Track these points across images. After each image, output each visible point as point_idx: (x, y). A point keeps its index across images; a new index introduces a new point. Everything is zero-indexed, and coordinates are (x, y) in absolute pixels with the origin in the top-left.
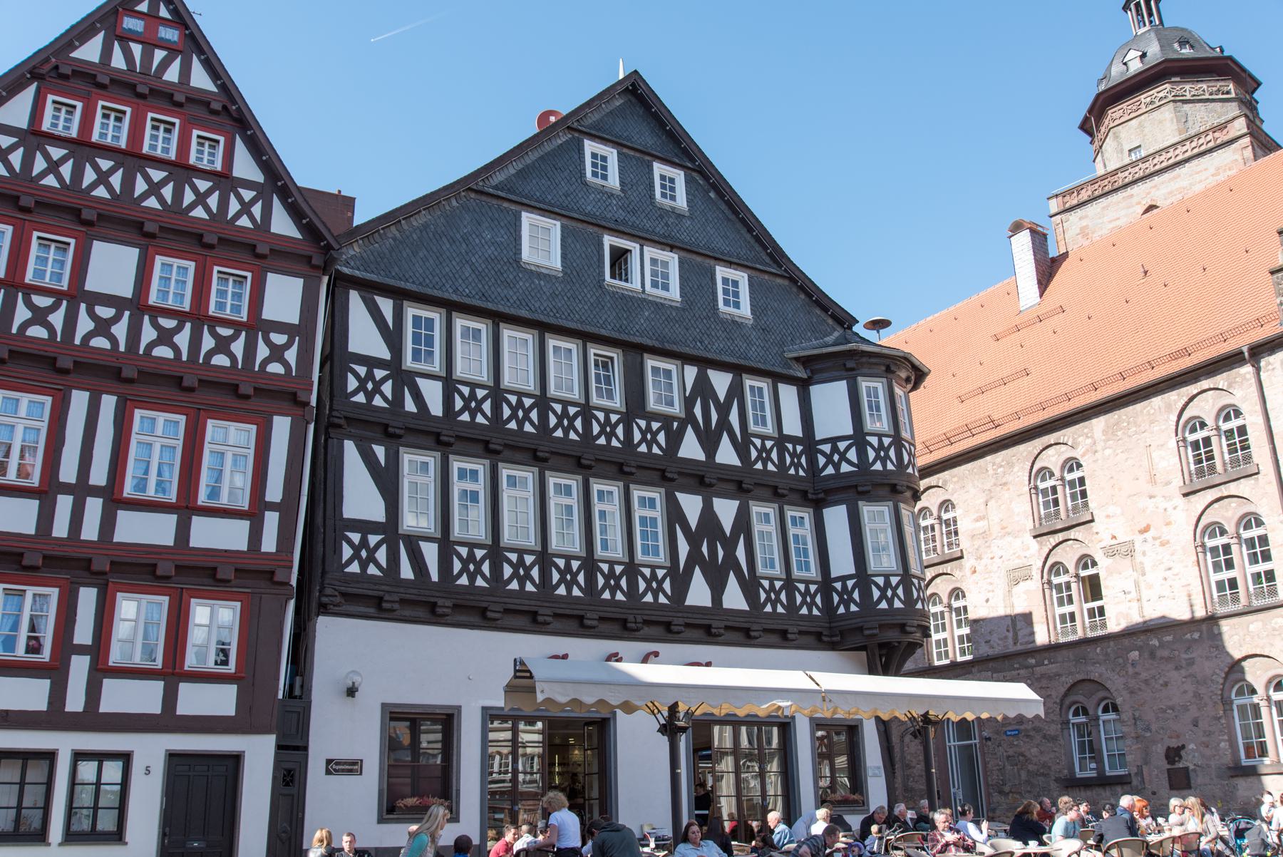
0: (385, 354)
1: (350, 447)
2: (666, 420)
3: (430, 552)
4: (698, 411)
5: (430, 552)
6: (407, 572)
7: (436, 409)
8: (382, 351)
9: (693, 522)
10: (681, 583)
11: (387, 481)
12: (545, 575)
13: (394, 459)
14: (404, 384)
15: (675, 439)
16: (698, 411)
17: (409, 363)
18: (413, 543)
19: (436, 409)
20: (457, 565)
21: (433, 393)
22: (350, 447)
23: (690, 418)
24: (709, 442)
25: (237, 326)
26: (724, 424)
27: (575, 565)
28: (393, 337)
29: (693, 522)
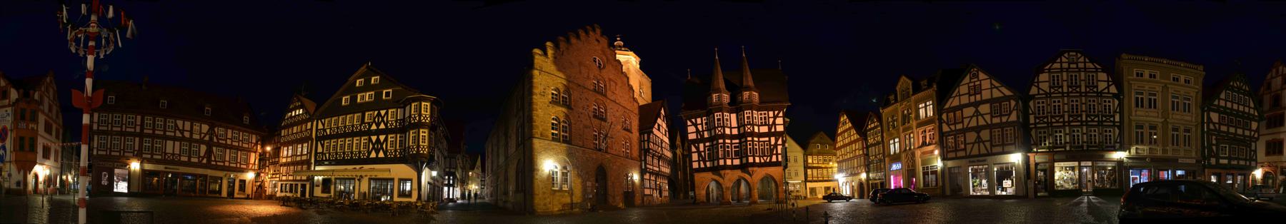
2: (369, 123)
4: (376, 120)
9: (374, 141)
10: (369, 153)
15: (370, 126)
16: (376, 120)
23: (374, 121)
24: (378, 125)
26: (383, 120)
29: (374, 141)
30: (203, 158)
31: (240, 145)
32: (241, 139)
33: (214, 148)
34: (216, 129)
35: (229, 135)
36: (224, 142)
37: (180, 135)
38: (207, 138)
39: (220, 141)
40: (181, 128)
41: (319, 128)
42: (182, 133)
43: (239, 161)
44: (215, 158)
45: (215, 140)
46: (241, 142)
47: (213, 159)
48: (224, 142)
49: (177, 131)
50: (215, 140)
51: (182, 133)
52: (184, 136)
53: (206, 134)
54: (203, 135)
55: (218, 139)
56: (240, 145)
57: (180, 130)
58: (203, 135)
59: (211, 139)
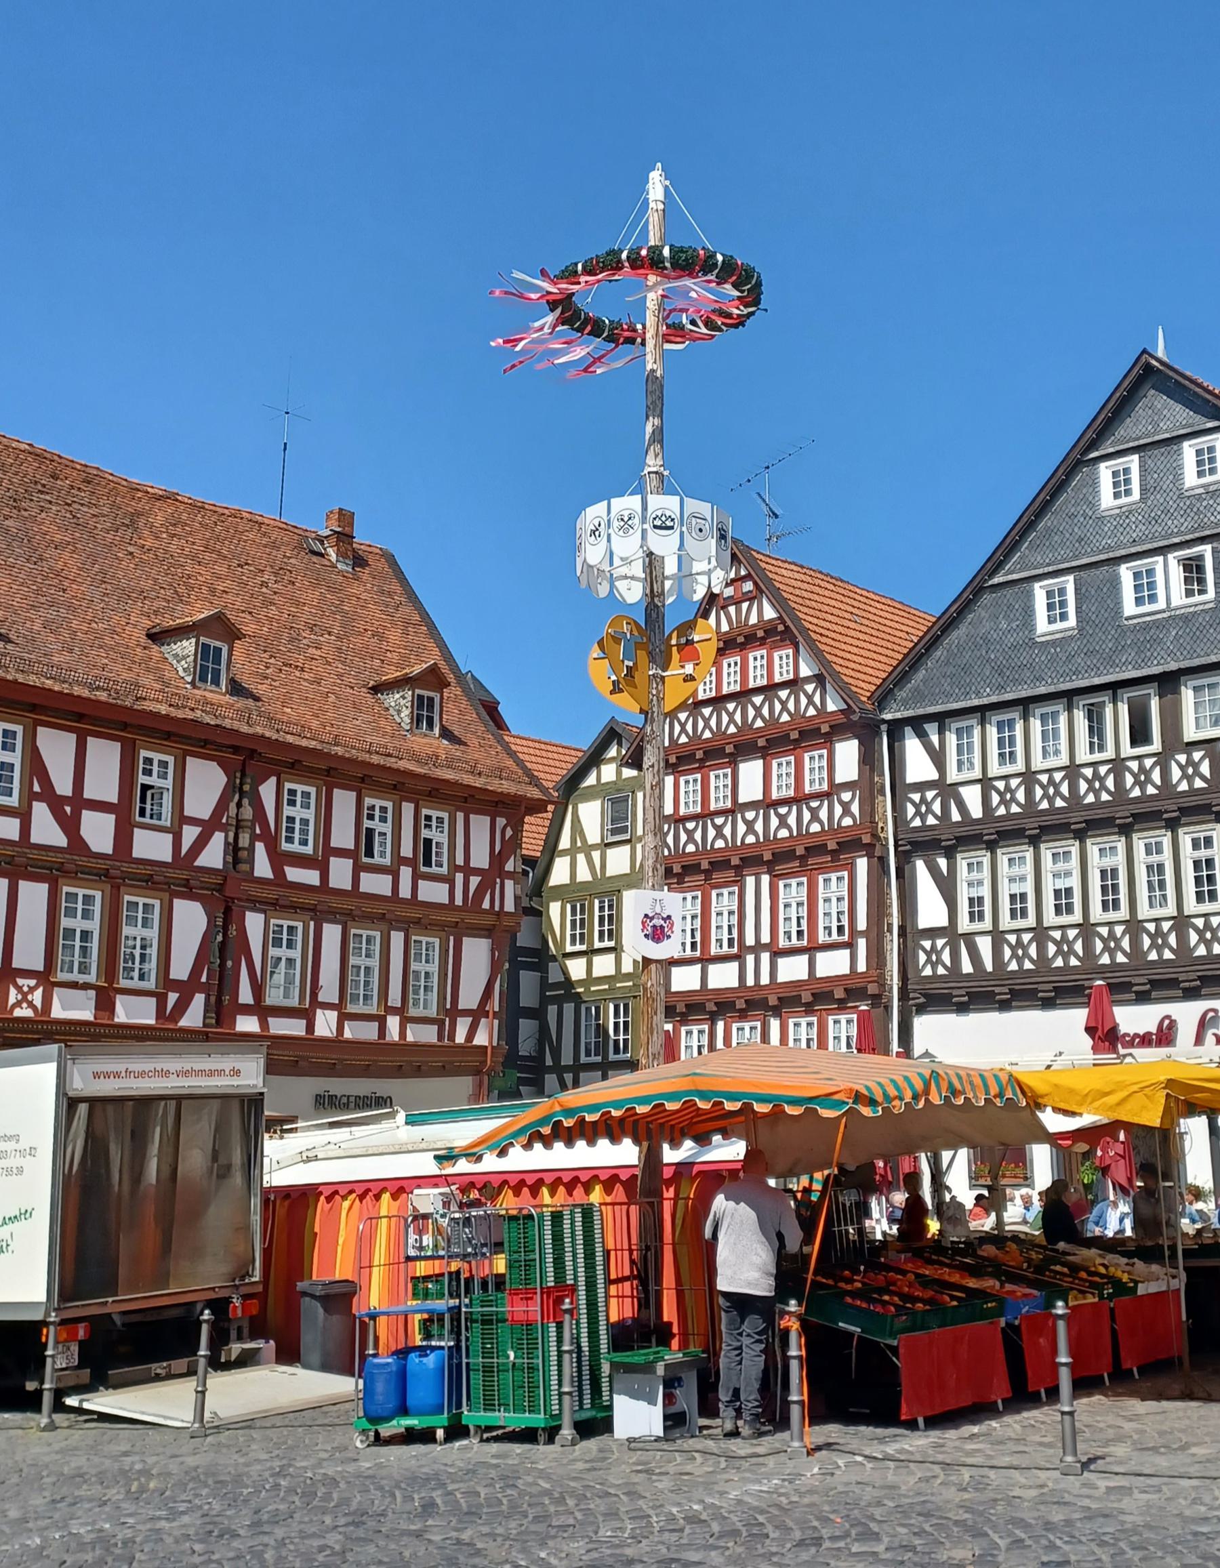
0: (932, 774)
1: (920, 865)
3: (985, 945)
5: (985, 945)
6: (967, 967)
7: (976, 812)
8: (932, 774)
11: (947, 888)
12: (1088, 946)
13: (952, 868)
14: (949, 796)
17: (953, 776)
18: (969, 937)
19: (976, 812)
20: (1007, 953)
21: (972, 797)
22: (920, 865)
25: (818, 796)
27: (1119, 930)
28: (938, 758)
30: (187, 989)
31: (405, 892)
32: (407, 850)
33: (254, 923)
34: (267, 791)
35: (343, 836)
36: (311, 877)
37: (61, 840)
38: (213, 856)
39: (294, 874)
40: (63, 786)
41: (912, 776)
42: (70, 825)
43: (395, 998)
44: (258, 989)
45: (262, 867)
46: (406, 873)
47: (246, 995)
48: (311, 877)
49: (41, 811)
50: (262, 867)
51: (70, 825)
52: (77, 842)
53: (208, 828)
54: (190, 834)
55: (279, 859)
56: (405, 892)
57: (56, 804)
58: (190, 834)
59: (234, 851)
